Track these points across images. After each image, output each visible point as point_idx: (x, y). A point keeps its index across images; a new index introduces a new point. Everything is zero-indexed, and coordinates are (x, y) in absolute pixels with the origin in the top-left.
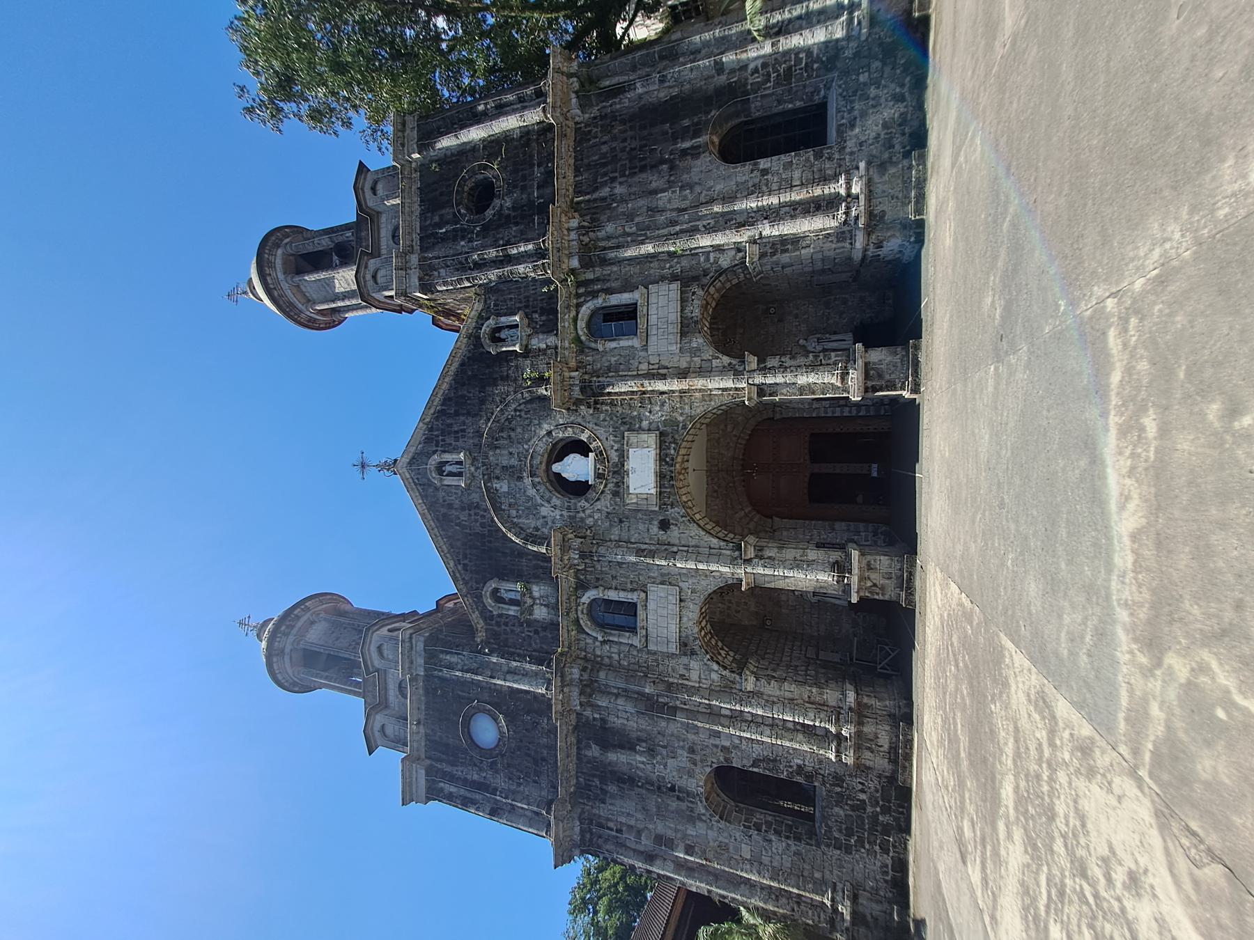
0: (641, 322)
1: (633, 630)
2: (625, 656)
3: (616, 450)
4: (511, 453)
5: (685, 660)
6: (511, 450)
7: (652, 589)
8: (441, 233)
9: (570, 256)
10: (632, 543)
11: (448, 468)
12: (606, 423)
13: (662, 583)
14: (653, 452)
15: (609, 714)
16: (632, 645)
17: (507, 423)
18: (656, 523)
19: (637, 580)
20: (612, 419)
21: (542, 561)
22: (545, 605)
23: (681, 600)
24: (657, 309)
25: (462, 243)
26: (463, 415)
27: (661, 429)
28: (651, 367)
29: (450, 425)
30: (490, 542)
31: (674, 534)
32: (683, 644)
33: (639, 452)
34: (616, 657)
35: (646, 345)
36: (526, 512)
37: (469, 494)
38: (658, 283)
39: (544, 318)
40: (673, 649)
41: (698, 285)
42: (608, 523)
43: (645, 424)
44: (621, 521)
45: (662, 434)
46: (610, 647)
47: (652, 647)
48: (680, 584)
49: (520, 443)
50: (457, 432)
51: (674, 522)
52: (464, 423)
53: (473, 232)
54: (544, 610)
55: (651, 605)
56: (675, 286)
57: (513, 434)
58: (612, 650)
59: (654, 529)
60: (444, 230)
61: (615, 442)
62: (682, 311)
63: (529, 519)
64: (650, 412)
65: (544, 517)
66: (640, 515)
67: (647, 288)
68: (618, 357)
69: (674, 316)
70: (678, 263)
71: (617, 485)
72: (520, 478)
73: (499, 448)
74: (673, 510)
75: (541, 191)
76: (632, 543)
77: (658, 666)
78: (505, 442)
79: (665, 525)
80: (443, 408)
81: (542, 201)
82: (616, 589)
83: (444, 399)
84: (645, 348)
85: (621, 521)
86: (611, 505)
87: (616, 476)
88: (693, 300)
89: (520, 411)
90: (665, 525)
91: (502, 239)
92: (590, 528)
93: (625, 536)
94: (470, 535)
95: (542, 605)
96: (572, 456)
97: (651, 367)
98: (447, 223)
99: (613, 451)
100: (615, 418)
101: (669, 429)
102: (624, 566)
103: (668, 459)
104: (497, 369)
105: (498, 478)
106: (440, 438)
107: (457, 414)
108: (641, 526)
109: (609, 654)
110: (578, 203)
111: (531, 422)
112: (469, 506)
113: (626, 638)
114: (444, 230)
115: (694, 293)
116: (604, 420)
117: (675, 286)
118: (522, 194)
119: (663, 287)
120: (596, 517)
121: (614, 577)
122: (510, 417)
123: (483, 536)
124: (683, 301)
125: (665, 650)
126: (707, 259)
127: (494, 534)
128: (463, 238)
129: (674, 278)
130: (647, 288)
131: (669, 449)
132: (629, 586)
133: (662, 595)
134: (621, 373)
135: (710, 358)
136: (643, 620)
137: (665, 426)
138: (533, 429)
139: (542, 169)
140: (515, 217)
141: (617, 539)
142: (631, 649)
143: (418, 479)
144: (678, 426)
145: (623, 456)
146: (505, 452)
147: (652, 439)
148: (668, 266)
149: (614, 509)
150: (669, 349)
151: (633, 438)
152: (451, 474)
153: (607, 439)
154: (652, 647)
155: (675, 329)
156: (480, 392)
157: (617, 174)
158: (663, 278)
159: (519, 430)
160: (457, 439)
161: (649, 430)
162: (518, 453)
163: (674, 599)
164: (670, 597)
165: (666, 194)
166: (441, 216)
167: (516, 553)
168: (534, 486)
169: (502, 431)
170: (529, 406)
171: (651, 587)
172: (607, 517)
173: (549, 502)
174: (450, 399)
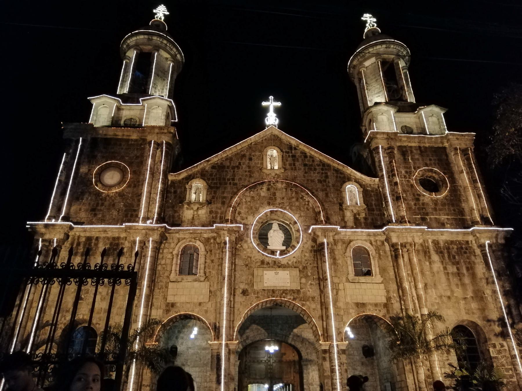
0: (362, 279)
1: (181, 272)
2: (164, 268)
3: (288, 263)
4: (283, 198)
5: (163, 307)
6: (285, 198)
7: (207, 285)
8: (408, 159)
9: (398, 237)
12: (303, 257)
13: (210, 291)
14: (289, 285)
15: (127, 258)
16: (171, 272)
17: (301, 196)
18: (247, 287)
19: (212, 276)
20: (306, 260)
21: (220, 217)
22: (193, 218)
23: (200, 304)
24: (370, 289)
25: (403, 172)
26: (305, 169)
27: (302, 291)
28: (337, 285)
29: (298, 161)
30: (230, 184)
31: (239, 298)
32: (173, 305)
33: (288, 276)
34: (163, 262)
35: (350, 282)
36: (249, 207)
37: (258, 171)
38: (385, 289)
39: (362, 220)
41: (385, 313)
42: (245, 258)
43: (303, 280)
44: (247, 265)
45: (298, 291)
46: (169, 258)
47: (171, 285)
48: (210, 303)
49: (290, 203)
50: (294, 165)
51: (247, 299)
52: (300, 169)
53: (410, 178)
54: (190, 217)
55: (196, 284)
56: (384, 300)
57: (294, 200)
58: (168, 260)
59: (243, 286)
60: (410, 161)
61: (292, 262)
63: (245, 208)
64: (311, 284)
65: (247, 218)
66: (250, 277)
68: (342, 265)
69: (366, 299)
70: (397, 301)
72: (269, 204)
73: (286, 191)
74: (254, 298)
75: (433, 219)
77: (159, 289)
78: (290, 195)
79: (244, 292)
80: (308, 157)
81: (429, 220)
82: (205, 262)
83: (313, 158)
84: (348, 280)
85: (247, 265)
86: (256, 259)
87: (273, 263)
88: (376, 310)
89: (308, 205)
90: (244, 292)
91: (407, 196)
92: (242, 246)
93: (238, 268)
94: (234, 171)
95: (194, 215)
96: (283, 235)
97: (337, 285)
98: (414, 163)
99: (287, 261)
100: (306, 262)
101: (301, 295)
102: (220, 267)
103: (284, 294)
104: (332, 190)
105: (268, 189)
106: (291, 154)
107: (305, 165)
108: (244, 278)
109: (164, 257)
110: (428, 242)
111: (302, 211)
112: (251, 171)
113: (175, 268)
114: (410, 161)
115: (380, 311)
116: (305, 256)
117: (384, 300)
118: (432, 208)
119: (383, 293)
120: (248, 250)
121: (212, 261)
122: (305, 198)
123: (233, 179)
124: (376, 305)
125: (169, 293)
127: (235, 186)
128: (406, 172)
129: (389, 299)
131: (290, 295)
132: (207, 270)
133: (203, 291)
134: (333, 266)
135: (344, 321)
136: (187, 279)
137: (303, 293)
138: (298, 212)
139: (446, 221)
140: (419, 204)
141: (236, 263)
142: (168, 272)
143: (266, 139)
144: (303, 301)
146: (284, 194)
147: (296, 286)
148: (395, 295)
149: (254, 261)
150: (348, 296)
151: (296, 272)
153: (294, 257)
154: (171, 285)
156: (318, 180)
157: (444, 265)
158: (388, 292)
159: (297, 204)
160: (290, 165)
161: (301, 283)
162: (283, 203)
164: (202, 297)
165: (435, 294)
166: (418, 160)
167: (224, 200)
169: (296, 193)
170: (311, 210)
171: (207, 284)
172: (249, 257)
174: (313, 161)
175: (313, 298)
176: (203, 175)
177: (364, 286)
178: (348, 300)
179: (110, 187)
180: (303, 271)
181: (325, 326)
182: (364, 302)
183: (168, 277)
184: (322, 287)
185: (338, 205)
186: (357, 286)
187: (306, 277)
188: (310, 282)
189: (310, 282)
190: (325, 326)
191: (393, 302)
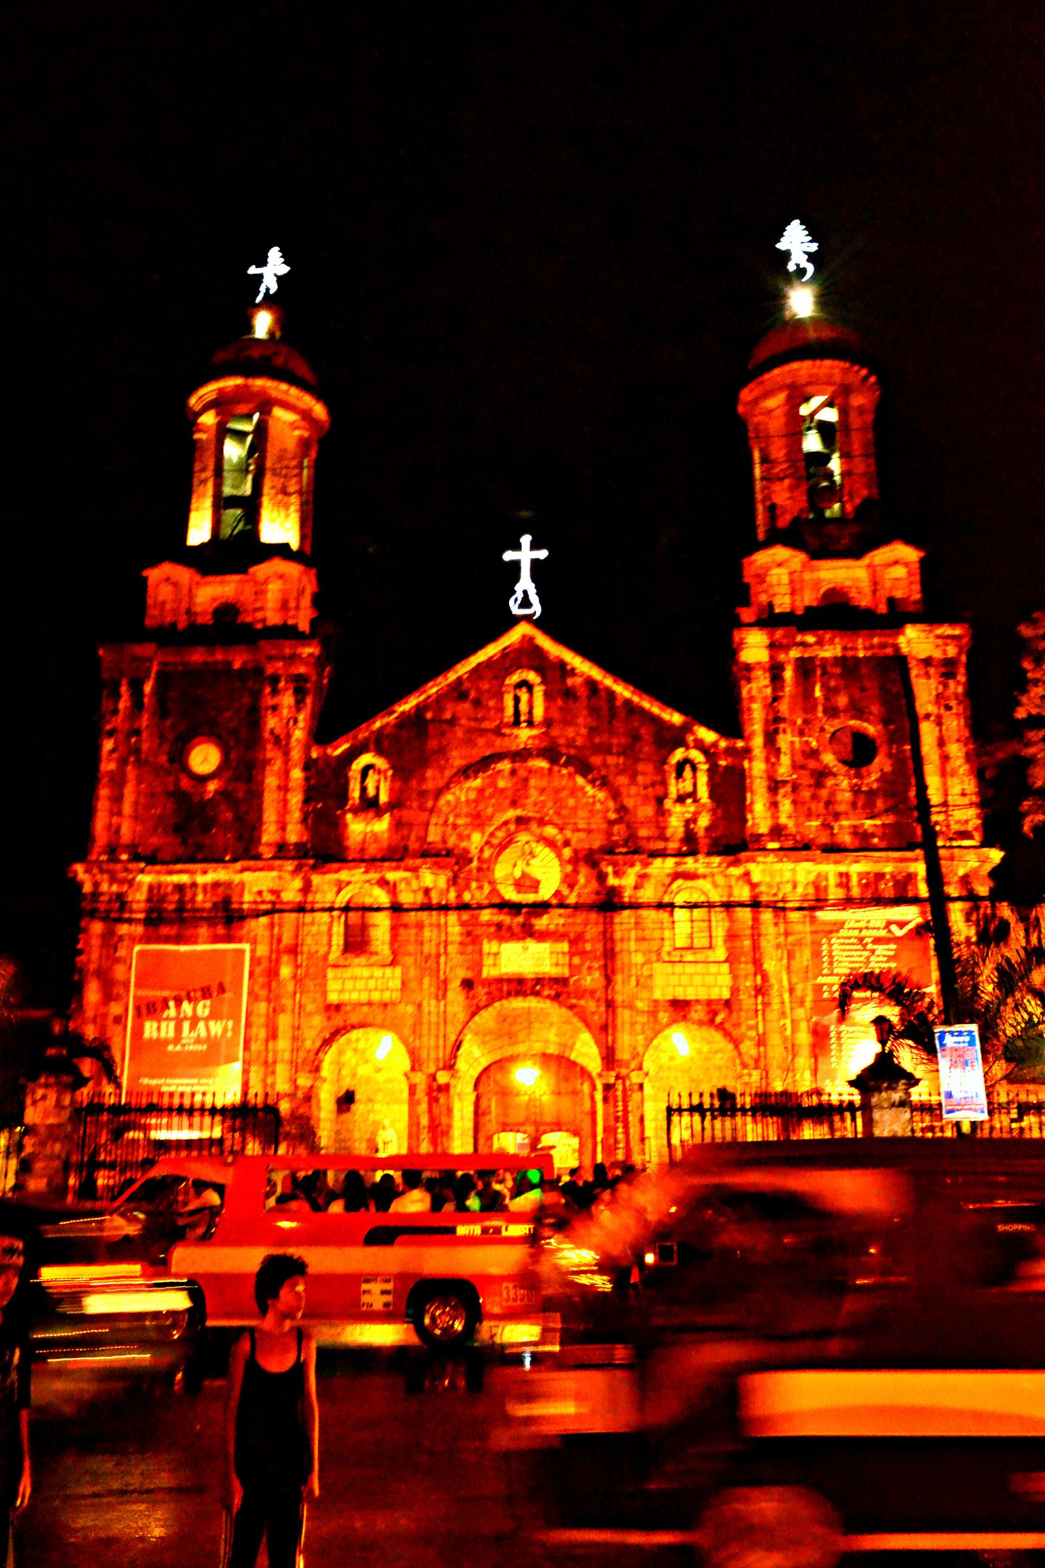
10: (446, 947)
11: (524, 697)
40: (333, 998)
62: (697, 1001)
67: (726, 961)
70: (750, 996)
71: (510, 928)
76: (446, 947)
101: (571, 989)
117: (726, 995)
119: (726, 980)
126: (750, 1028)
129: (735, 990)
130: (726, 961)
145: (542, 936)
152: (517, 700)
154: (331, 973)
155: (680, 994)
163: (387, 996)
168: (506, 823)
173: (487, 843)
175: (592, 993)
176: (378, 744)
177: (690, 969)
178: (657, 995)
179: (205, 779)
180: (576, 941)
181: (610, 1044)
182: (688, 998)
183: (325, 957)
184: (609, 972)
185: (653, 802)
186: (679, 968)
187: (583, 953)
188: (587, 964)
189: (587, 964)
190: (610, 1044)
191: (742, 997)
